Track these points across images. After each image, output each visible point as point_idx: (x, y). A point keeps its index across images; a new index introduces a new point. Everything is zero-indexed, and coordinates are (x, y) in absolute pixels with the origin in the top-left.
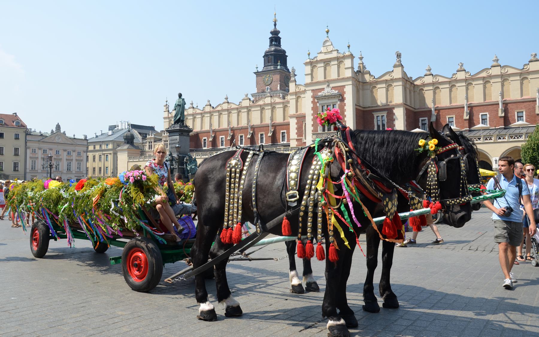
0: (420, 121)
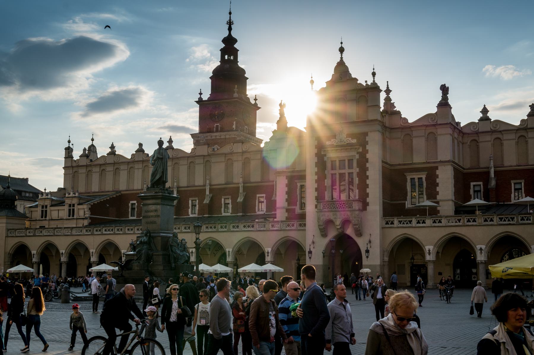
0: (472, 187)
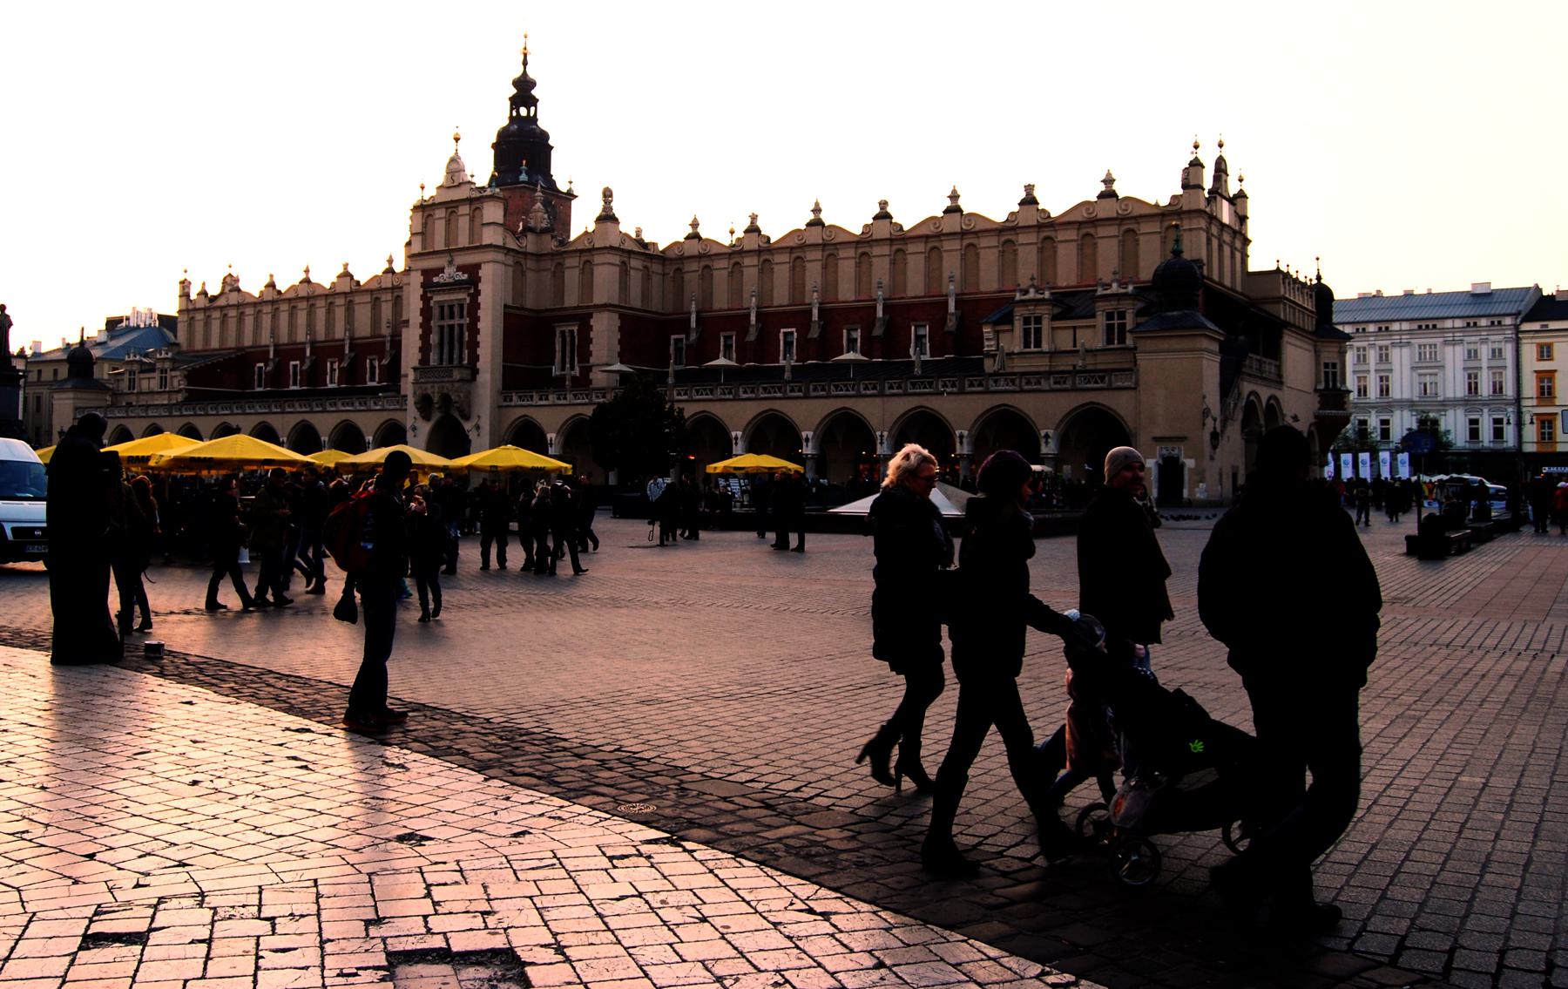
0: (672, 342)
